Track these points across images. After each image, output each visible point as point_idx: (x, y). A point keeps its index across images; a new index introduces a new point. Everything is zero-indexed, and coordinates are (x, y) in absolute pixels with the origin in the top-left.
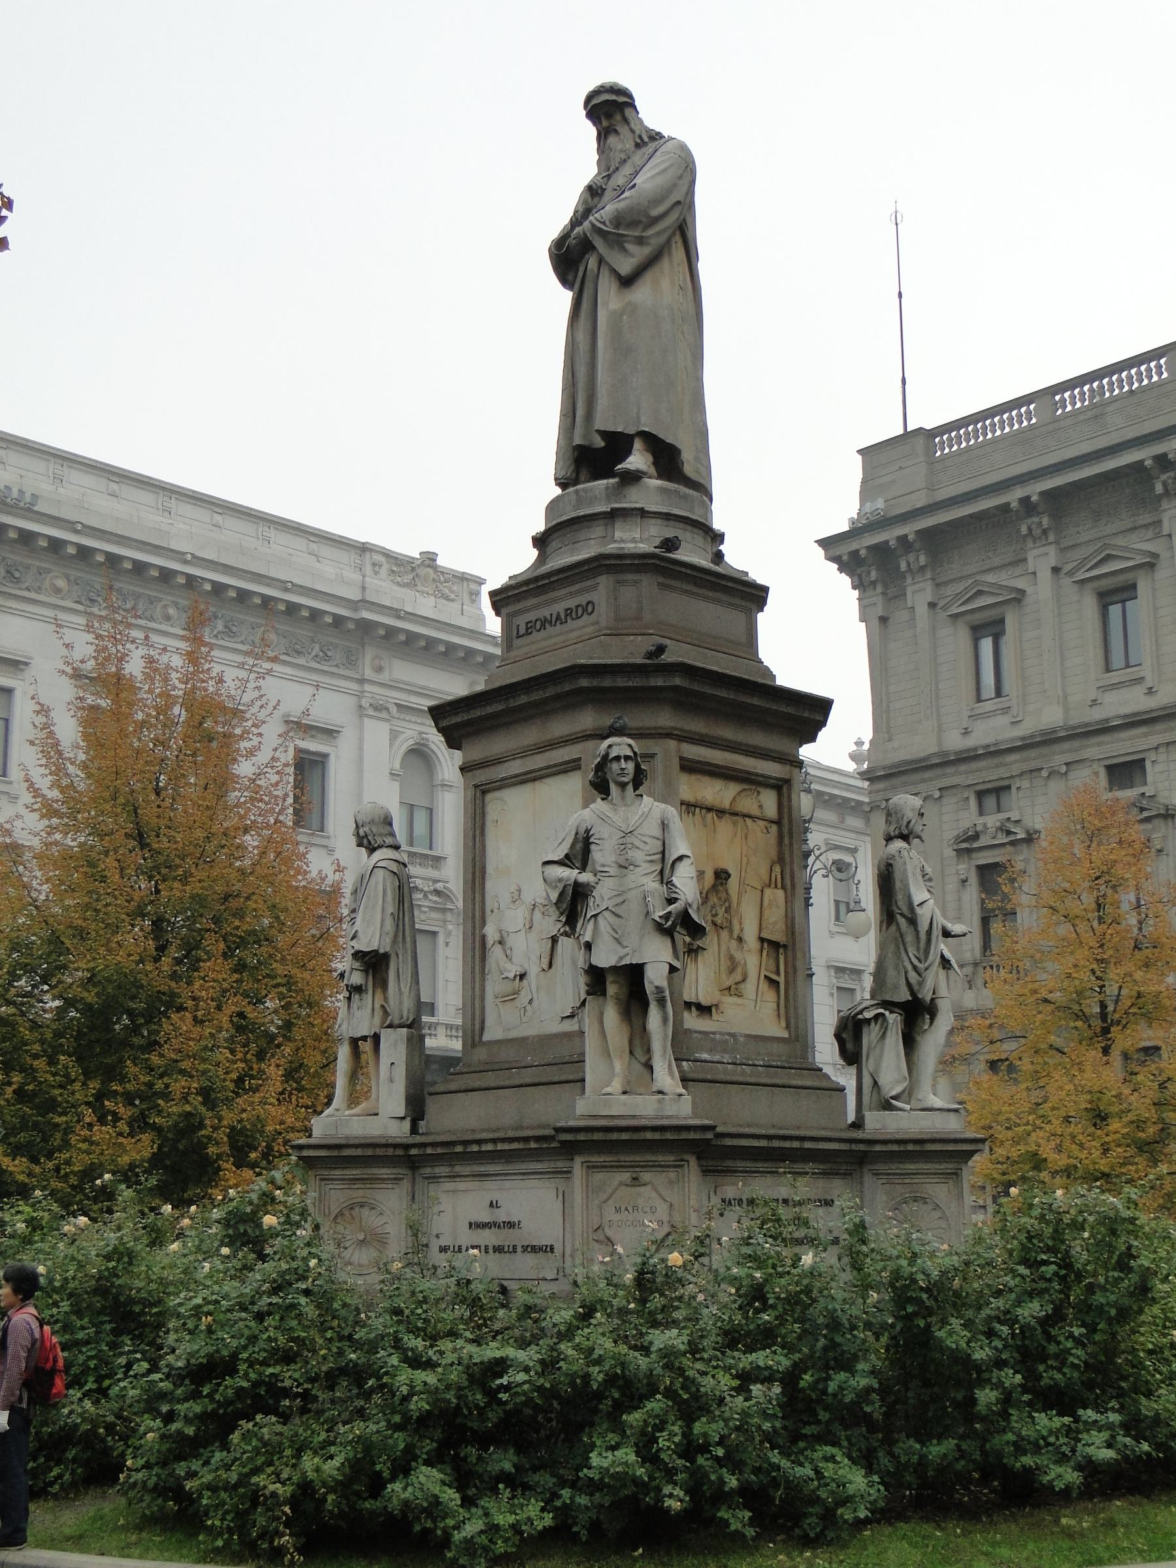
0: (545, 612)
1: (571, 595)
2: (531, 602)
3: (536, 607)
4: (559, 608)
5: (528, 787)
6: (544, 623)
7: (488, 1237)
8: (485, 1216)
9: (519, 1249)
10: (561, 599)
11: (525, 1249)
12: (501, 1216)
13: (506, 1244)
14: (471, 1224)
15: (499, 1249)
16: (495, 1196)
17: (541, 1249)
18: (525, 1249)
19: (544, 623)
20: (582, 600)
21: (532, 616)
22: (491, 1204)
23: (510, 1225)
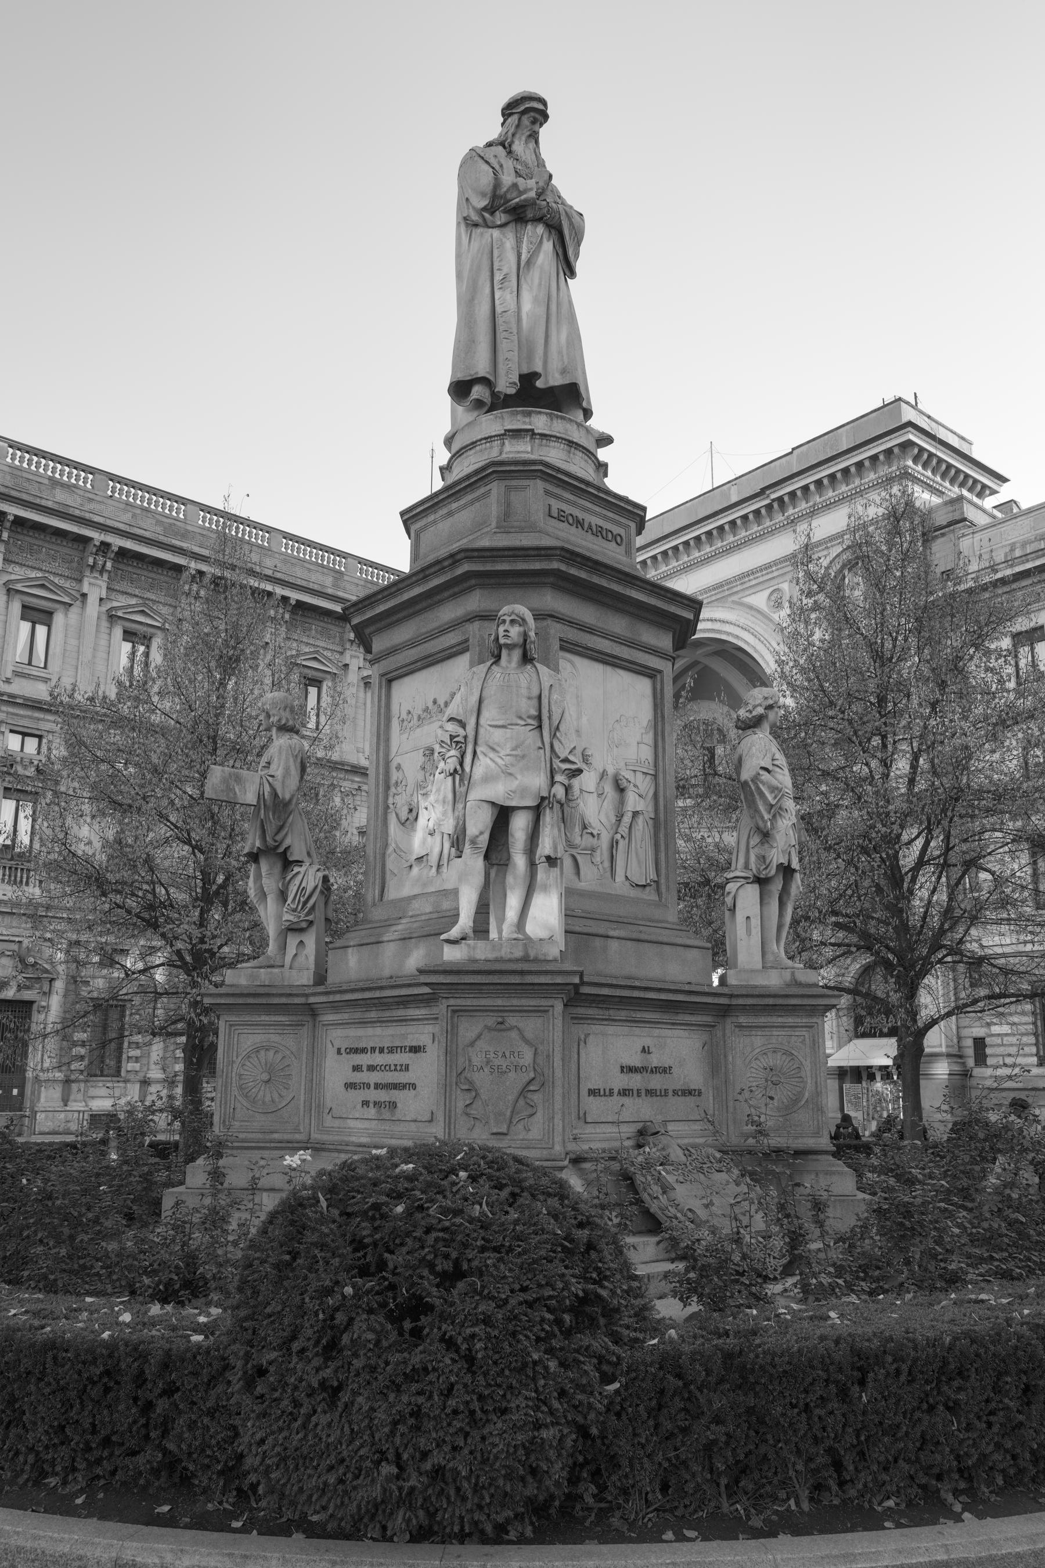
0: (580, 517)
1: (605, 518)
2: (567, 495)
3: (574, 504)
4: (595, 521)
5: (599, 667)
6: (579, 523)
7: (635, 1081)
8: (636, 1061)
9: (671, 1093)
10: (595, 514)
11: (675, 1093)
12: (654, 1060)
13: (658, 1087)
14: (622, 1068)
15: (650, 1093)
16: (648, 1042)
17: (690, 1093)
18: (675, 1093)
19: (579, 523)
20: (616, 530)
21: (564, 507)
22: (644, 1050)
23: (665, 1070)
